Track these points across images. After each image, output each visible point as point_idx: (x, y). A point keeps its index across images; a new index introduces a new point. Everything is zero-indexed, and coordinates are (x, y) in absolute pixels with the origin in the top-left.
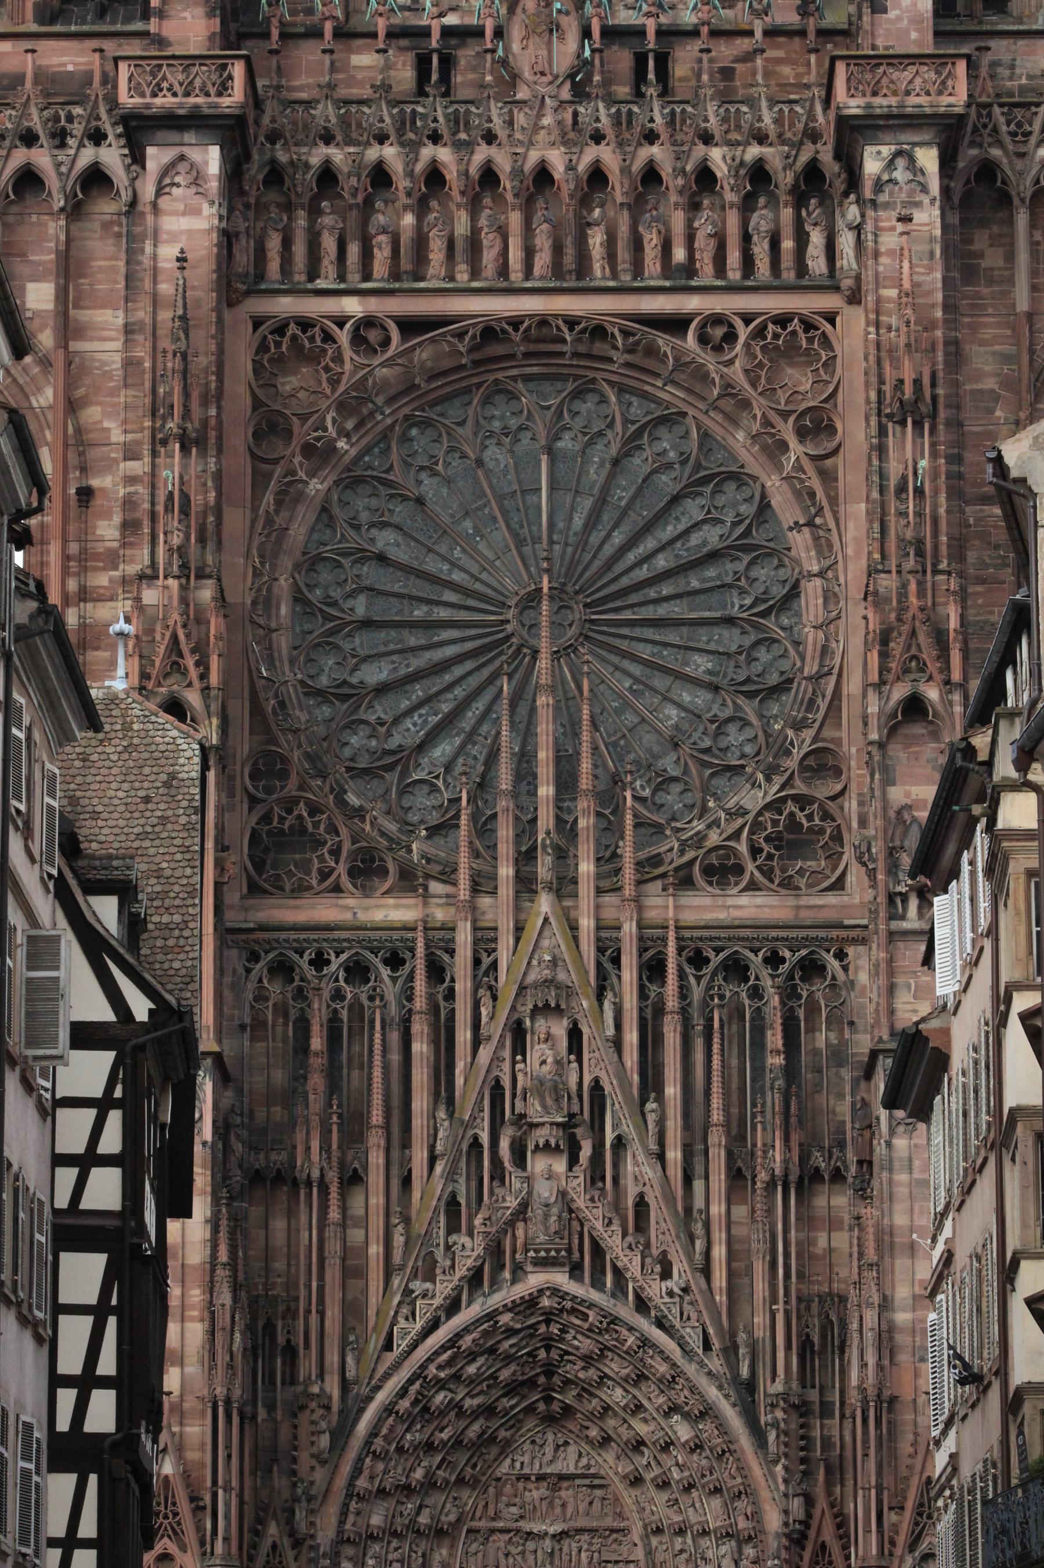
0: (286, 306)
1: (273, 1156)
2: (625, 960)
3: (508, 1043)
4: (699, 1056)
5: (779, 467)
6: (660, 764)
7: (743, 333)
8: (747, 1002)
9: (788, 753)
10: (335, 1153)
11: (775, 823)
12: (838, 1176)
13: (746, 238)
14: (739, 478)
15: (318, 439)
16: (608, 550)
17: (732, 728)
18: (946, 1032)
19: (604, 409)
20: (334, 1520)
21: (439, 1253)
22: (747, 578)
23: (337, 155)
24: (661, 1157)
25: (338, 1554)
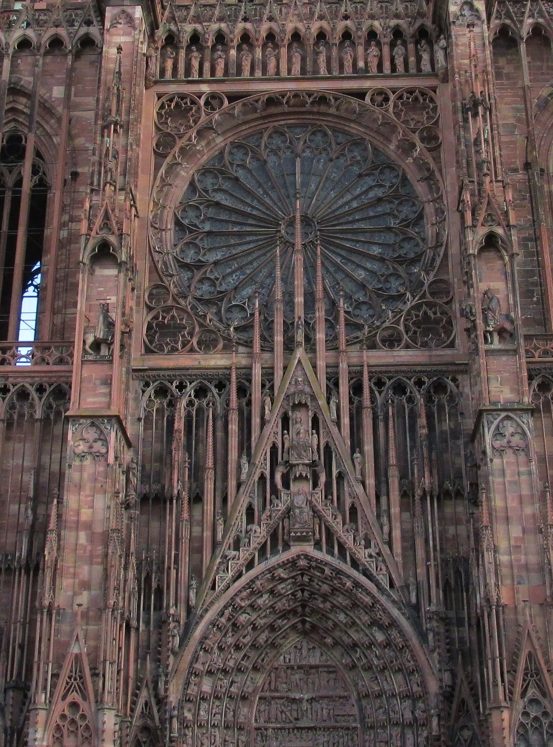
0: (173, 89)
2: (341, 381)
3: (280, 425)
4: (381, 431)
7: (392, 97)
9: (423, 284)
10: (187, 486)
11: (417, 316)
12: (459, 494)
13: (392, 60)
14: (391, 167)
15: (187, 146)
17: (392, 279)
20: (181, 687)
22: (398, 211)
23: (199, 27)
24: (363, 483)
25: (182, 708)
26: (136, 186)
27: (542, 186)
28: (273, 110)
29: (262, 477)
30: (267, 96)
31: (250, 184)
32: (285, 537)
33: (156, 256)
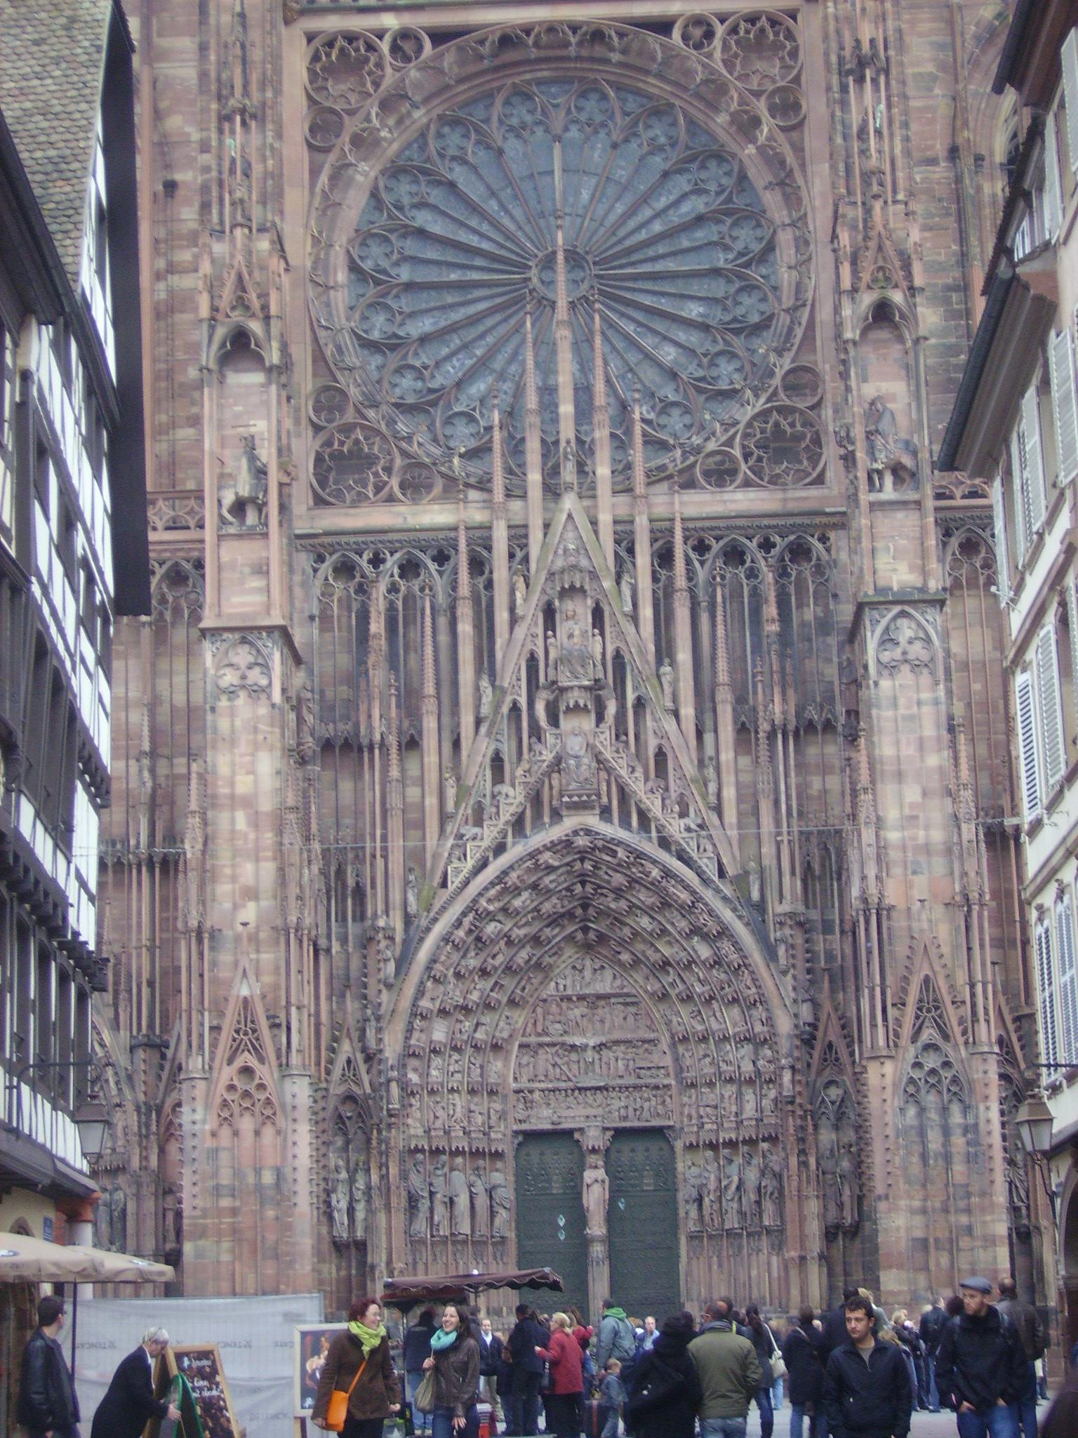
0: (332, 23)
1: (341, 726)
2: (638, 548)
5: (753, 140)
6: (661, 394)
7: (720, 30)
8: (745, 581)
9: (772, 374)
11: (763, 431)
12: (829, 726)
14: (720, 156)
15: (364, 130)
16: (612, 218)
17: (722, 362)
18: (1051, 277)
19: (604, 105)
20: (400, 1036)
21: (487, 801)
24: (676, 714)
25: (404, 1066)
26: (281, 212)
27: (979, 189)
28: (511, 56)
29: (515, 708)
30: (498, 35)
31: (474, 191)
32: (555, 803)
33: (322, 334)
